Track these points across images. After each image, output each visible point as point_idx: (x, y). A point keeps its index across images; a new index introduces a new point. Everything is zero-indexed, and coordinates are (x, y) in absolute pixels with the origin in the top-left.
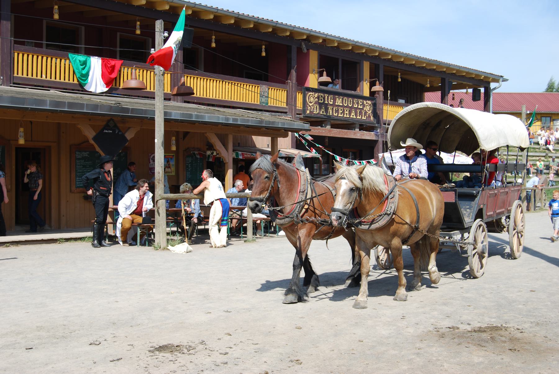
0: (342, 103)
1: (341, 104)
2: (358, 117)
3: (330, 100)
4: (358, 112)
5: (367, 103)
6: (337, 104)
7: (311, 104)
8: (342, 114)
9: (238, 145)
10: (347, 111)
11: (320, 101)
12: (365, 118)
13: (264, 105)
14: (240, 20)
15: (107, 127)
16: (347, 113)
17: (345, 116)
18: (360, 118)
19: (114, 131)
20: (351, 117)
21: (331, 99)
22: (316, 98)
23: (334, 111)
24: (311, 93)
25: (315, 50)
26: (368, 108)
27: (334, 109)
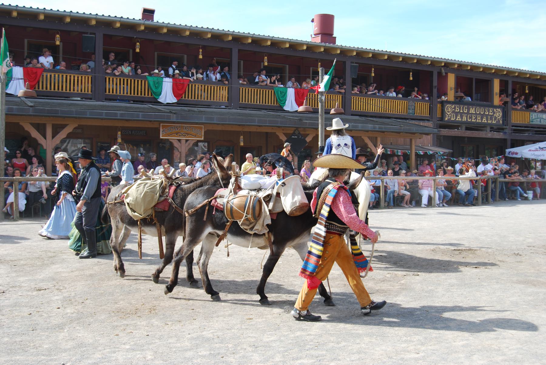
0: (475, 111)
1: (474, 112)
2: (489, 122)
3: (464, 109)
5: (497, 111)
6: (470, 112)
7: (448, 113)
9: (390, 144)
11: (456, 111)
12: (495, 122)
13: (411, 115)
14: (392, 57)
15: (294, 134)
17: (478, 121)
18: (491, 122)
19: (298, 137)
20: (483, 121)
21: (465, 109)
22: (453, 108)
23: (468, 118)
24: (449, 105)
25: (452, 73)
26: (498, 114)
27: (468, 116)
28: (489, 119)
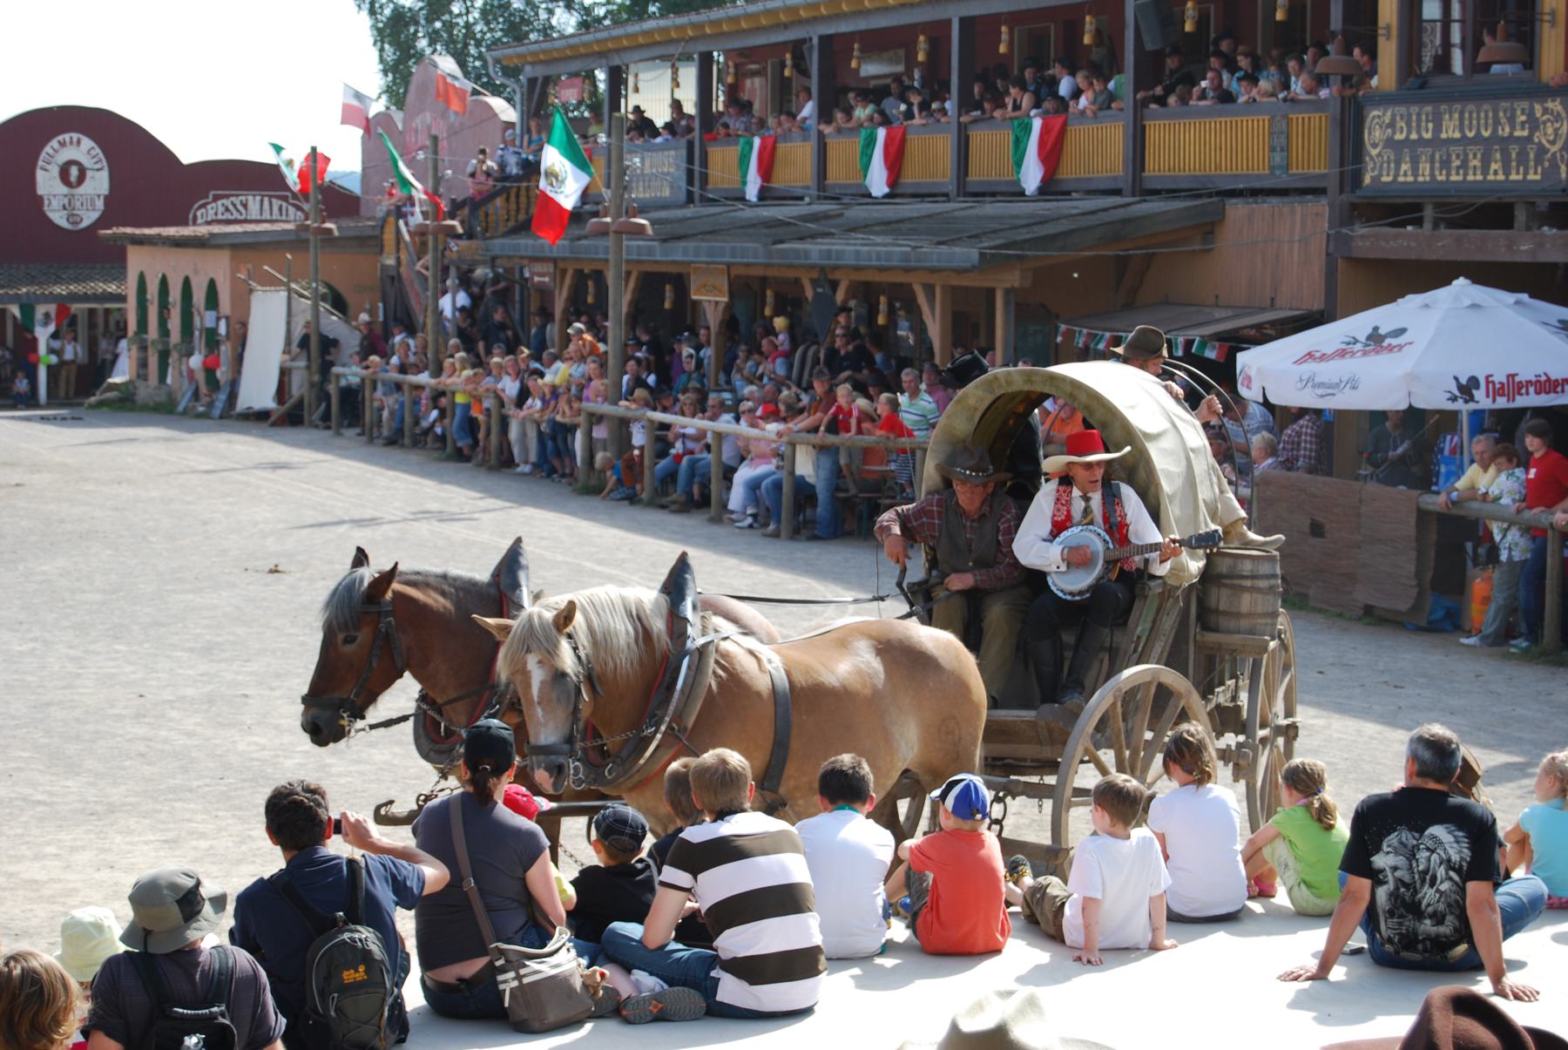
0: (1462, 131)
1: (1457, 135)
2: (1513, 177)
3: (1423, 124)
4: (1514, 155)
5: (1545, 111)
6: (1444, 136)
8: (1461, 172)
10: (1475, 157)
11: (1398, 137)
16: (1475, 167)
17: (1470, 178)
20: (1491, 177)
21: (1427, 121)
23: (1437, 165)
26: (1550, 131)
27: (1437, 157)
28: (1514, 164)
